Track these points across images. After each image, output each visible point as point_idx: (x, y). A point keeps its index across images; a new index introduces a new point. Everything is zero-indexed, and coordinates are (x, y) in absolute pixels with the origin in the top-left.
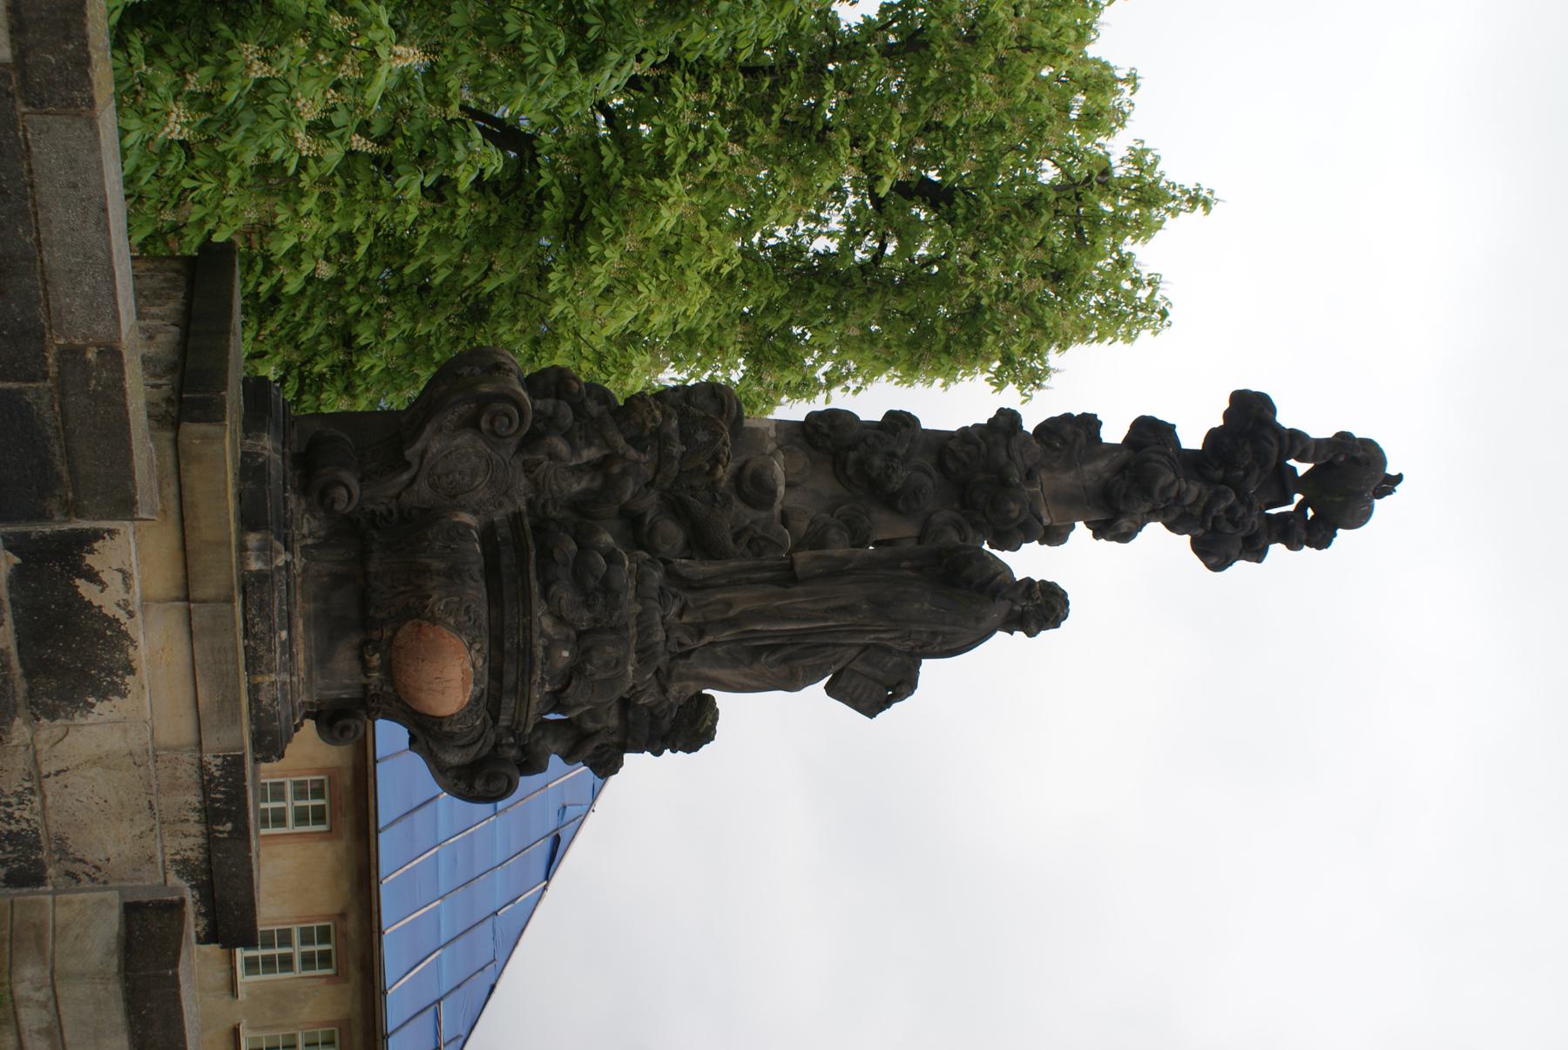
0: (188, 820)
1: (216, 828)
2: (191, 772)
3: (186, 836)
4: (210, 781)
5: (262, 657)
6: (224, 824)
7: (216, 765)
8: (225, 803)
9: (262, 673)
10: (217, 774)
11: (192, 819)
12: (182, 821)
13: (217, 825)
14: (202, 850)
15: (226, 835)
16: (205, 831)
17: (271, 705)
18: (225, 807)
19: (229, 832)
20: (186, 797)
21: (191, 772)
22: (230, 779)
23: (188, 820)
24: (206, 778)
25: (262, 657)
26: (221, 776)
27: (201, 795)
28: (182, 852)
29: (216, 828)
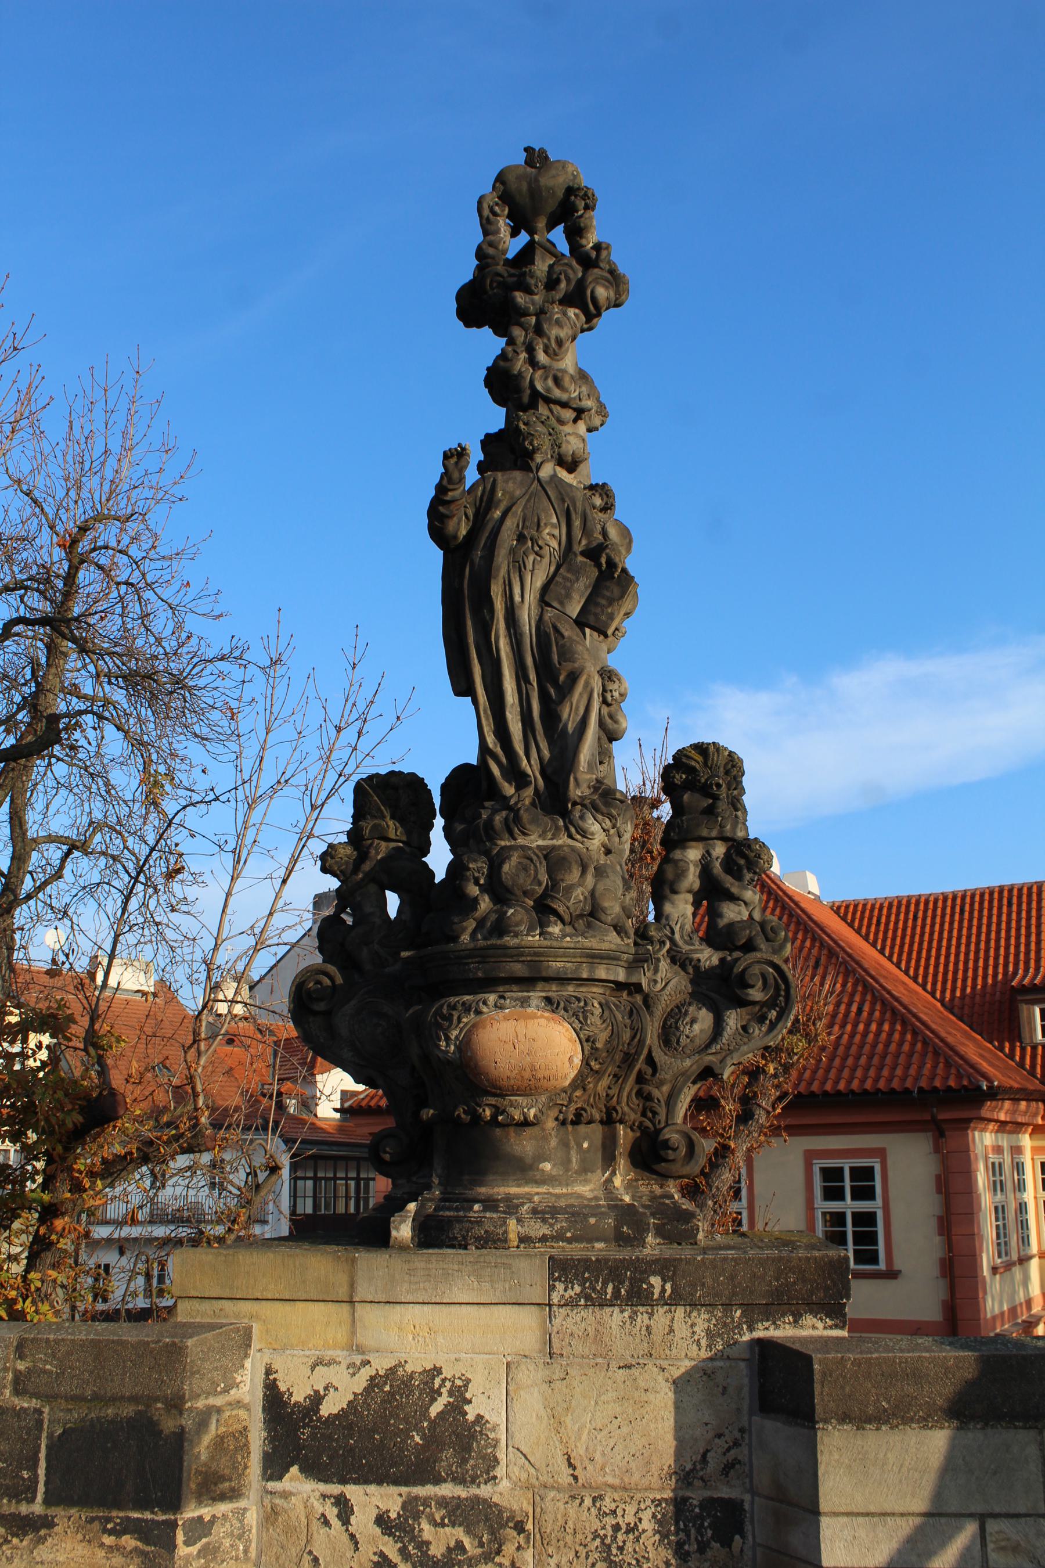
0: (648, 1327)
1: (656, 1296)
2: (578, 1318)
3: (672, 1331)
4: (588, 1298)
5: (486, 1231)
6: (652, 1286)
7: (566, 1290)
8: (622, 1282)
9: (506, 1232)
10: (577, 1289)
11: (646, 1322)
12: (650, 1334)
13: (653, 1293)
14: (695, 1314)
15: (668, 1286)
16: (666, 1308)
17: (552, 1225)
18: (627, 1283)
19: (664, 1281)
20: (613, 1326)
21: (578, 1318)
22: (587, 1275)
23: (648, 1327)
24: (582, 1302)
25: (486, 1231)
26: (582, 1285)
27: (611, 1309)
28: (696, 1337)
29: (656, 1296)
